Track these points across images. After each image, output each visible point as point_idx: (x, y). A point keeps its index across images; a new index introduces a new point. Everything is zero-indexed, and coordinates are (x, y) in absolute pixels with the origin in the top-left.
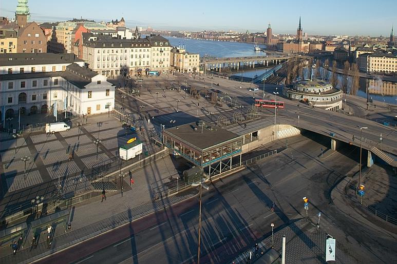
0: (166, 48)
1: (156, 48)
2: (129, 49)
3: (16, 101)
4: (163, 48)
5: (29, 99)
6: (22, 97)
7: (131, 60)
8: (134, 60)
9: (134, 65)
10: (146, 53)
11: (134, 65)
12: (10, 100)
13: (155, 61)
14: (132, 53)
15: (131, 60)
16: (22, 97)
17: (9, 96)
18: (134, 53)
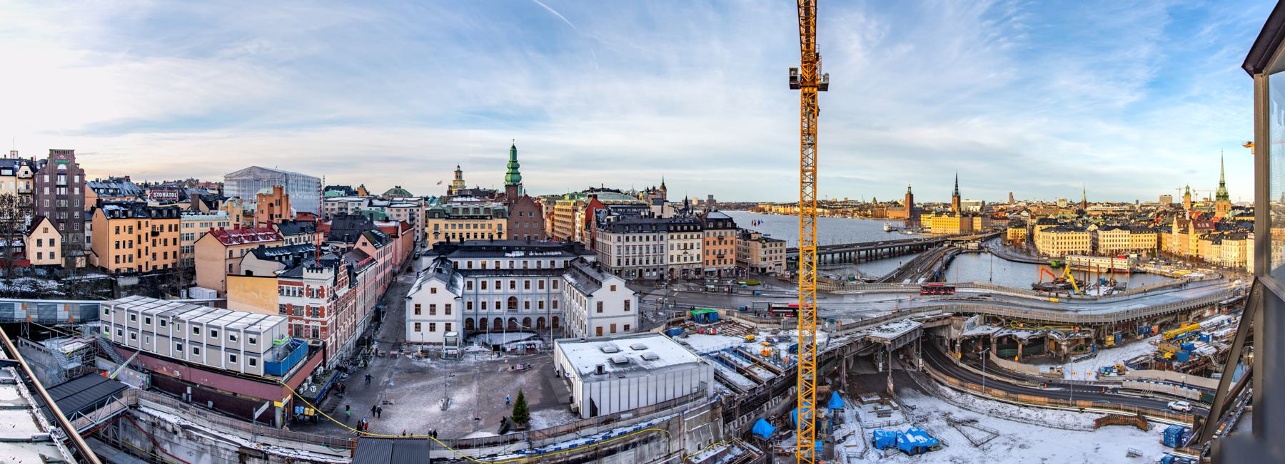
0: (729, 232)
1: (711, 232)
2: (666, 236)
3: (504, 305)
4: (723, 232)
5: (521, 306)
6: (512, 303)
7: (671, 253)
8: (676, 253)
9: (675, 261)
10: (695, 242)
11: (675, 261)
12: (498, 306)
13: (711, 253)
14: (671, 242)
15: (671, 253)
16: (512, 303)
17: (496, 300)
18: (675, 242)
